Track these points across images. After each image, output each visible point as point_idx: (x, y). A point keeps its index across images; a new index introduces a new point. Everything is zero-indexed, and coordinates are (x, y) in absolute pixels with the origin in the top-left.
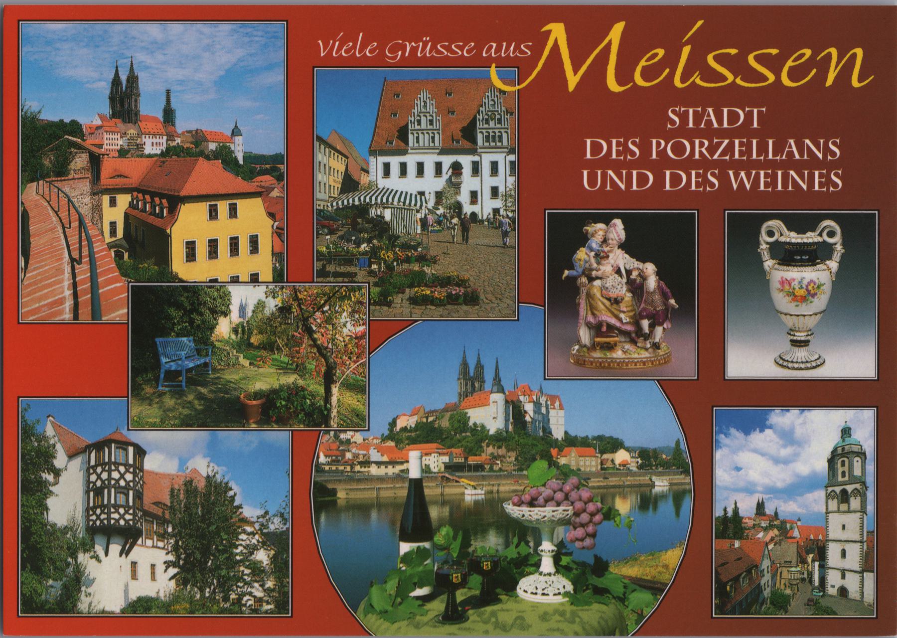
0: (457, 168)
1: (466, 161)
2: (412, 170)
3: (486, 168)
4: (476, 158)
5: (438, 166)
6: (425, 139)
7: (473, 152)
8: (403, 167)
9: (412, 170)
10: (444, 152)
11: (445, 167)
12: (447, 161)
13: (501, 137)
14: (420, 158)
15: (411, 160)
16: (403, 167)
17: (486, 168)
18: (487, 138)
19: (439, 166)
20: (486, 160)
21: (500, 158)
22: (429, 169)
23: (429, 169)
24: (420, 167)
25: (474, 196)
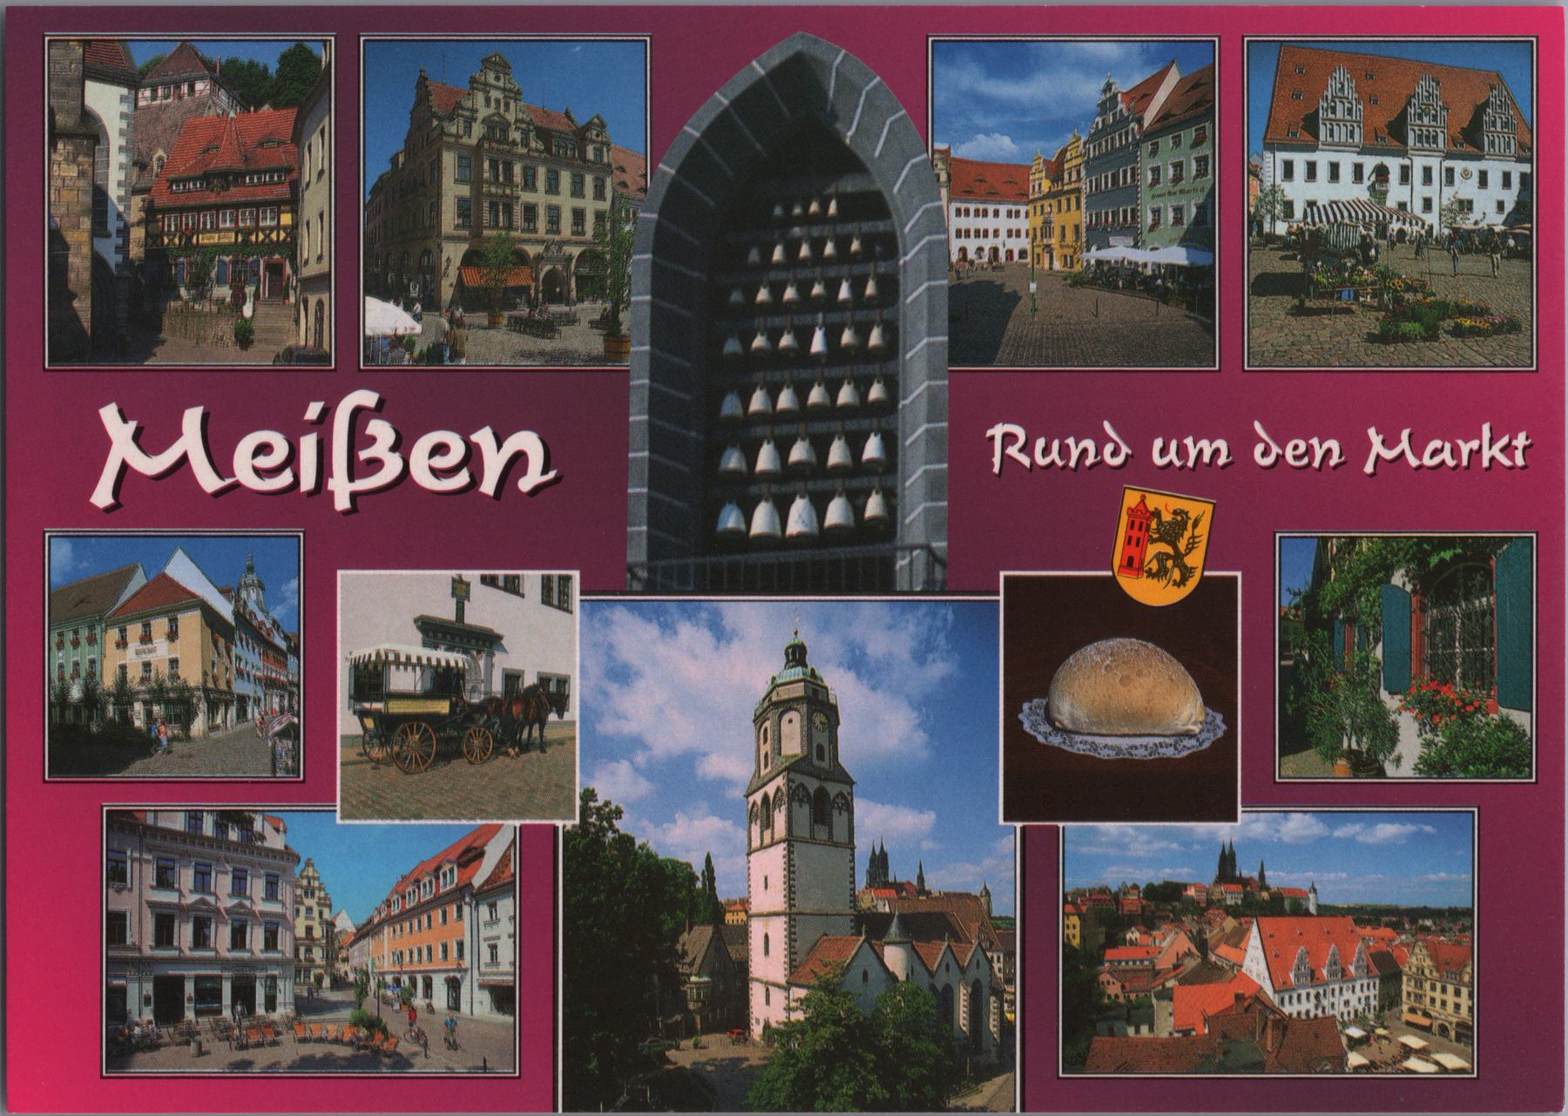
0: (1382, 173)
1: (1394, 164)
2: (1323, 172)
3: (1417, 175)
4: (1406, 162)
5: (1358, 170)
6: (1341, 134)
11: (1367, 171)
12: (1370, 163)
13: (1435, 138)
14: (1334, 157)
15: (1322, 159)
17: (1417, 175)
18: (1420, 136)
20: (1419, 163)
21: (1434, 163)
23: (1346, 172)
24: (1334, 170)
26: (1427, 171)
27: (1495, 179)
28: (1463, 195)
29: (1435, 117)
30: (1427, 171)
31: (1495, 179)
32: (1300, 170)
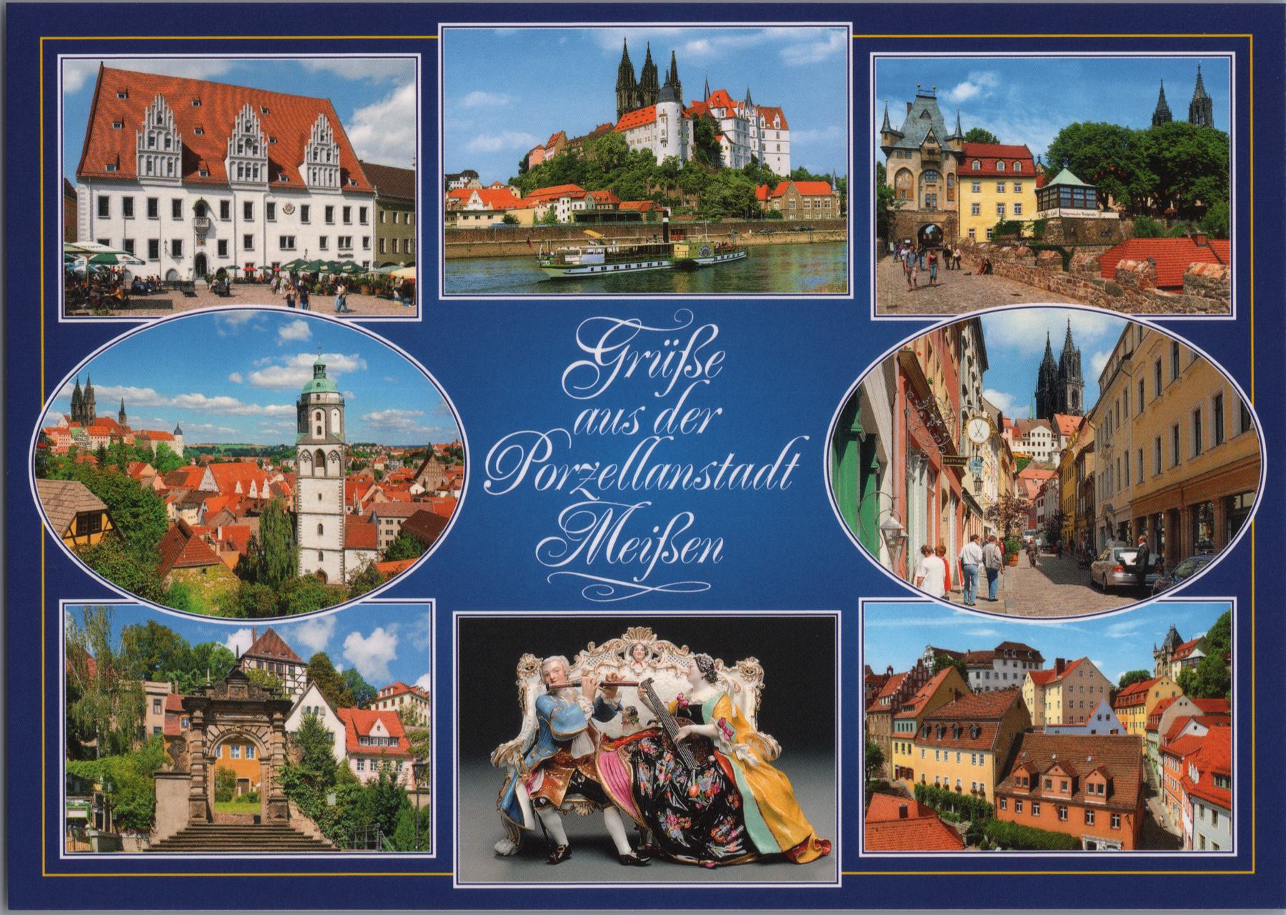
4: (225, 198)
6: (161, 166)
7: (224, 186)
8: (128, 206)
9: (140, 208)
10: (188, 185)
12: (189, 199)
13: (256, 170)
16: (128, 206)
17: (237, 210)
18: (240, 169)
19: (177, 205)
20: (238, 200)
22: (165, 209)
23: (165, 209)
25: (222, 247)
26: (248, 207)
27: (317, 213)
28: (288, 233)
29: (256, 148)
30: (248, 207)
31: (317, 213)
32: (116, 206)
